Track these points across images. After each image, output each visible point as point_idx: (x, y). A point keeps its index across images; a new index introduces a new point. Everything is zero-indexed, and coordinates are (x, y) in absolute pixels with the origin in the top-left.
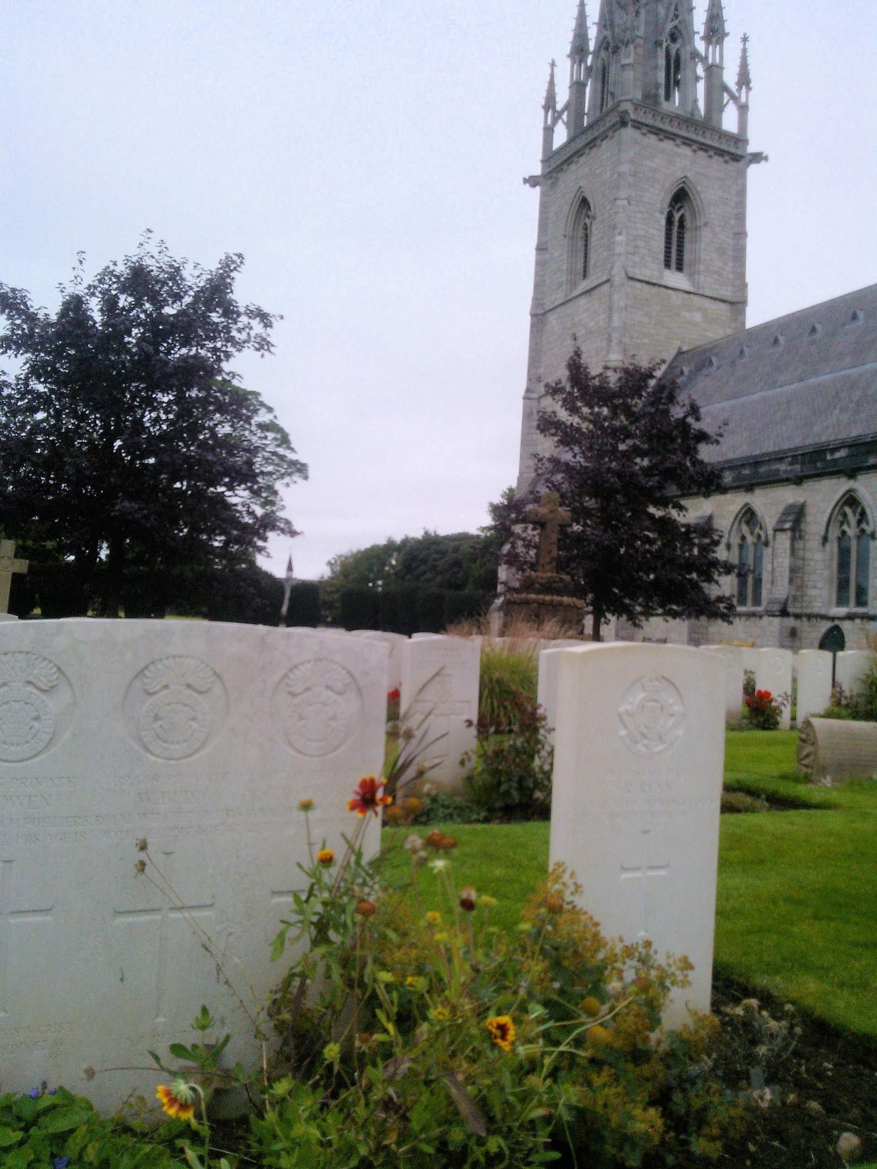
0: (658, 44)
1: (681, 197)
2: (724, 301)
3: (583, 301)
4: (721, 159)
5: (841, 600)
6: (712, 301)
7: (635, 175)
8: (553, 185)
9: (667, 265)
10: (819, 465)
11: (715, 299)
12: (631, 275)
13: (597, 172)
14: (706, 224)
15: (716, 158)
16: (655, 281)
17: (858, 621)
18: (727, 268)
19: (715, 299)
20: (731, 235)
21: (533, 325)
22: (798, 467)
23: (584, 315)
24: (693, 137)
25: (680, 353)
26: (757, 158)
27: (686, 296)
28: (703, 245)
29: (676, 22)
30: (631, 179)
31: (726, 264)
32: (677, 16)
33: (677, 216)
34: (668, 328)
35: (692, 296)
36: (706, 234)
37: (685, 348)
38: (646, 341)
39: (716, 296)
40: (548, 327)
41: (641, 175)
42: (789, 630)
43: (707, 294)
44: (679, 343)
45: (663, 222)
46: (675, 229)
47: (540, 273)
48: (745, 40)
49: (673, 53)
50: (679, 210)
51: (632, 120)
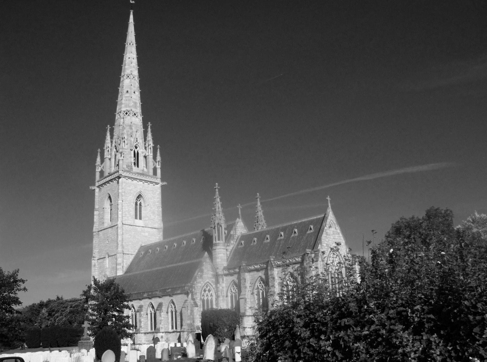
0: (131, 150)
1: (139, 196)
2: (155, 228)
3: (110, 230)
5: (173, 328)
6: (151, 229)
9: (136, 218)
10: (165, 293)
11: (152, 228)
12: (124, 223)
13: (113, 189)
16: (132, 224)
17: (175, 333)
19: (152, 228)
20: (156, 208)
22: (161, 293)
23: (110, 234)
24: (143, 179)
25: (141, 247)
27: (143, 228)
29: (137, 143)
31: (155, 217)
32: (137, 141)
33: (139, 203)
35: (144, 228)
37: (143, 245)
38: (131, 243)
39: (153, 227)
40: (100, 236)
41: (126, 192)
42: (161, 336)
43: (149, 227)
44: (140, 243)
45: (134, 206)
46: (138, 207)
49: (136, 152)
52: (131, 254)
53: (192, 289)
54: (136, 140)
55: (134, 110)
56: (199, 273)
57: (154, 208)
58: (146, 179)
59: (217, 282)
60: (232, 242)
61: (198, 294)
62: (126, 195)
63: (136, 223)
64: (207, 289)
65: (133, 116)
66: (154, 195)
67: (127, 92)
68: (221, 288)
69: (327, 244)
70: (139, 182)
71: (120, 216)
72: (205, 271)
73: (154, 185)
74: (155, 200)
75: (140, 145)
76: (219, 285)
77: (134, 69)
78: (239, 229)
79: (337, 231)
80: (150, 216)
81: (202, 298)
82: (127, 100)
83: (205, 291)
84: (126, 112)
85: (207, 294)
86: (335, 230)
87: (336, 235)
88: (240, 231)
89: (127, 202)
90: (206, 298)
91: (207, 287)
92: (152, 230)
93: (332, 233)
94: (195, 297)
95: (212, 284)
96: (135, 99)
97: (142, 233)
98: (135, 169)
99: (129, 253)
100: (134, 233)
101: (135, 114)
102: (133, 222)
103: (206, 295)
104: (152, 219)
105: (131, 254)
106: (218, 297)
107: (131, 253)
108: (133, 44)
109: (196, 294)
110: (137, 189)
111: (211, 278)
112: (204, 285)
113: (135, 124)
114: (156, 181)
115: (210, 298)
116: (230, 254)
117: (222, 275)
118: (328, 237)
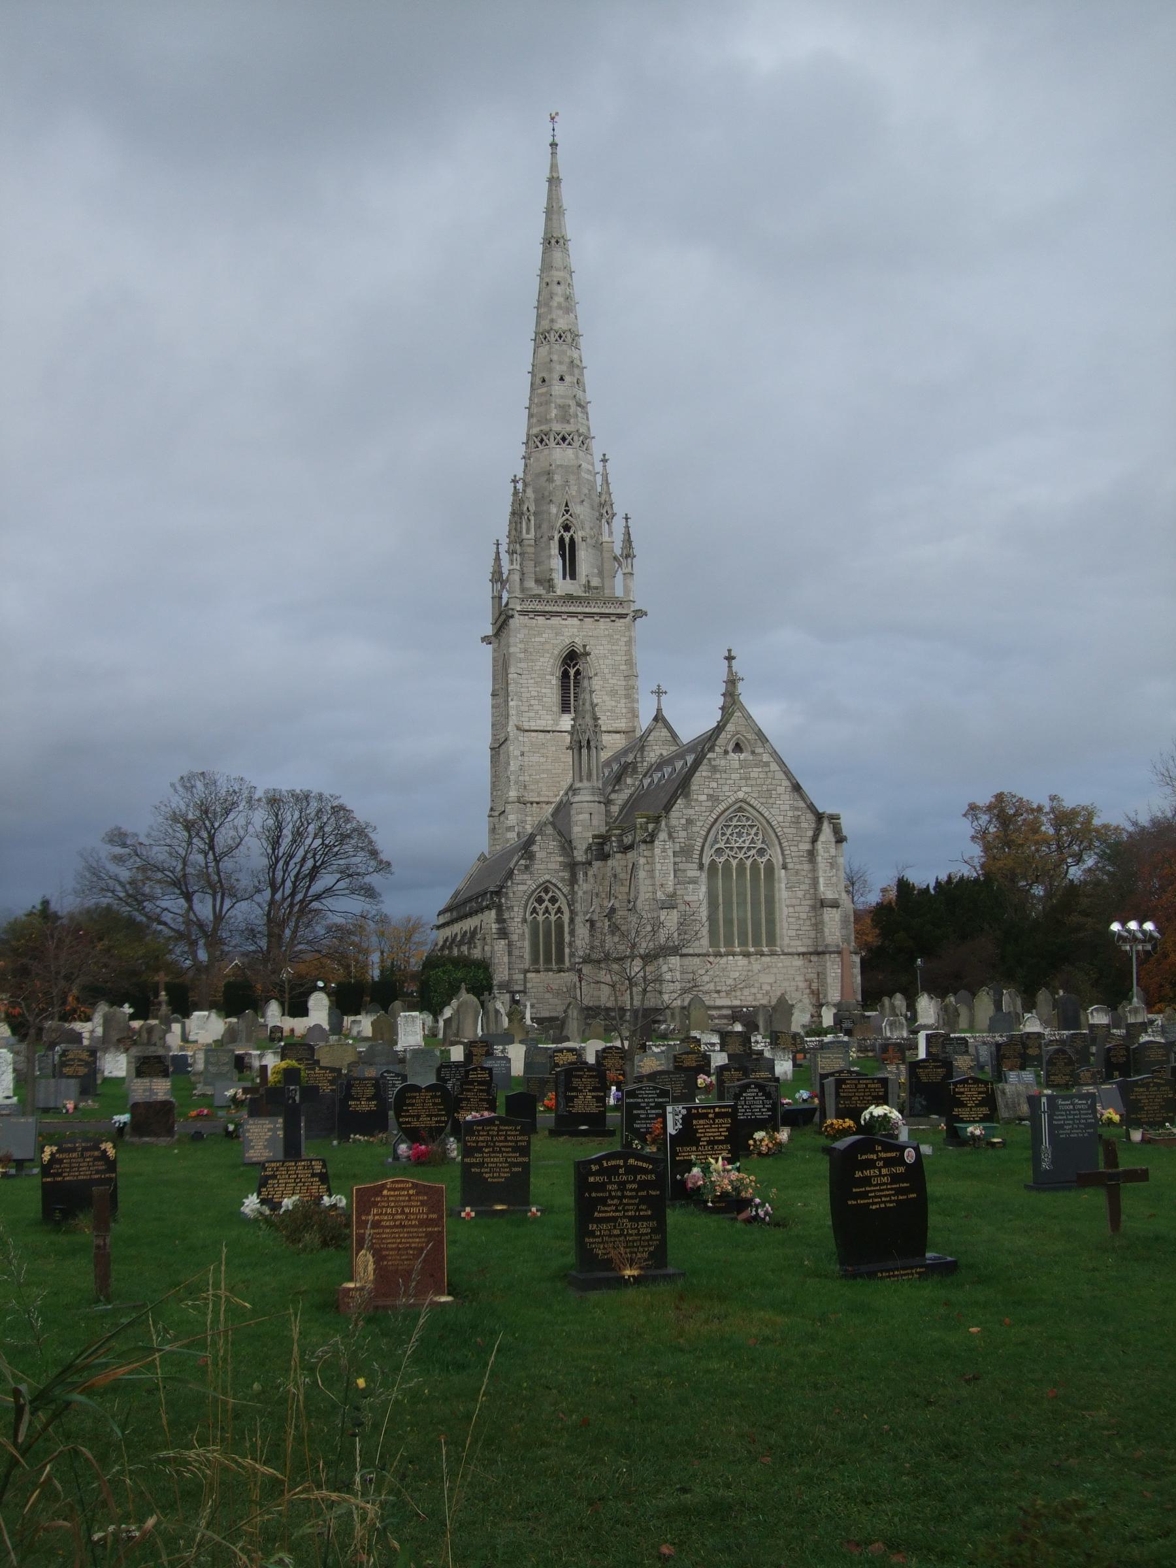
1: (572, 655)
4: (608, 620)
7: (525, 651)
8: (499, 643)
12: (527, 728)
14: (596, 675)
15: (602, 620)
16: (549, 729)
20: (622, 678)
21: (492, 757)
24: (579, 610)
26: (640, 614)
30: (522, 655)
32: (567, 511)
33: (572, 672)
34: (564, 762)
36: (596, 683)
39: (611, 729)
45: (555, 681)
47: (496, 714)
48: (627, 519)
49: (567, 540)
52: (548, 803)
53: (500, 899)
54: (563, 508)
55: (557, 427)
56: (522, 862)
57: (615, 682)
58: (587, 610)
59: (573, 881)
60: (629, 781)
61: (516, 909)
63: (561, 723)
64: (547, 898)
66: (614, 648)
67: (544, 381)
68: (580, 893)
69: (710, 797)
71: (512, 712)
72: (538, 855)
74: (618, 658)
75: (575, 522)
76: (576, 887)
77: (560, 312)
78: (654, 747)
79: (760, 758)
81: (529, 918)
82: (541, 405)
83: (540, 901)
84: (539, 438)
85: (547, 907)
86: (751, 758)
88: (658, 753)
89: (533, 676)
90: (541, 918)
91: (546, 891)
92: (610, 738)
93: (737, 766)
94: (506, 916)
95: (560, 885)
96: (562, 397)
99: (542, 799)
100: (554, 749)
101: (564, 439)
102: (552, 722)
103: (541, 912)
104: (610, 708)
105: (548, 803)
106: (573, 913)
107: (546, 799)
108: (557, 242)
109: (510, 908)
110: (562, 638)
111: (556, 871)
112: (536, 890)
113: (558, 466)
114: (619, 611)
115: (553, 918)
116: (621, 811)
117: (583, 864)
118: (718, 776)
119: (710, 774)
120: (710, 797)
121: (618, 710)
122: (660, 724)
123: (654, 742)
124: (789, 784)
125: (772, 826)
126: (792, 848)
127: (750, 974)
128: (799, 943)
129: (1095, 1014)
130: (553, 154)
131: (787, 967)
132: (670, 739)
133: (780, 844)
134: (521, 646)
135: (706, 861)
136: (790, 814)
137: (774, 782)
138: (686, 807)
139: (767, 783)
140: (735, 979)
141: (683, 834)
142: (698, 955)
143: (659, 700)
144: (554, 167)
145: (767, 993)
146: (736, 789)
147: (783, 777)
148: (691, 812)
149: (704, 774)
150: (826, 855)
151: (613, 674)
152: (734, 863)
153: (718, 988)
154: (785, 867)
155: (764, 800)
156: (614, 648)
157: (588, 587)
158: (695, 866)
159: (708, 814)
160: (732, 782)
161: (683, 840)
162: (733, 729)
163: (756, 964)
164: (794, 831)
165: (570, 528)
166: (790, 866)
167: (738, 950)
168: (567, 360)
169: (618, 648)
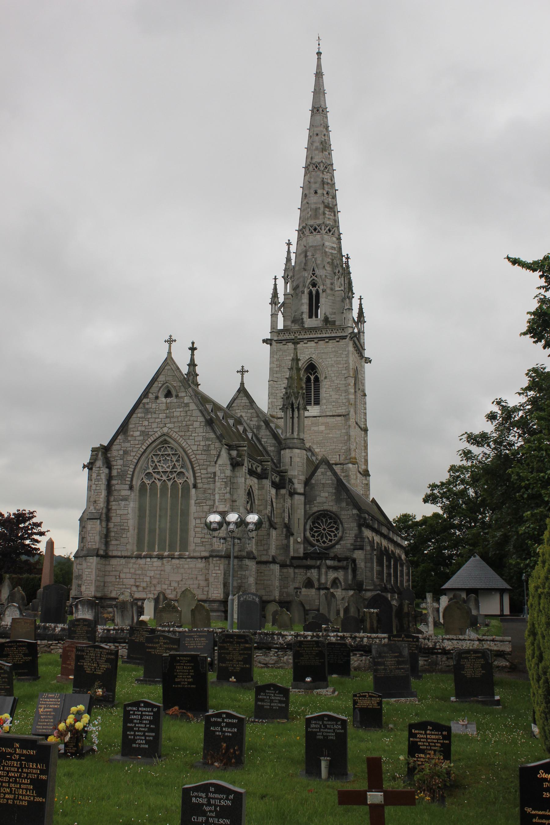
4: (334, 341)
14: (326, 378)
15: (331, 341)
18: (341, 397)
20: (343, 379)
27: (315, 418)
28: (325, 389)
30: (278, 369)
32: (314, 274)
33: (312, 378)
35: (318, 418)
39: (335, 414)
43: (328, 414)
49: (314, 292)
50: (314, 374)
51: (275, 341)
54: (311, 272)
57: (339, 382)
62: (283, 370)
65: (312, 233)
66: (338, 359)
69: (142, 432)
70: (309, 343)
73: (338, 341)
74: (341, 366)
75: (318, 280)
78: (237, 411)
80: (331, 396)
86: (175, 401)
87: (178, 410)
93: (164, 408)
96: (316, 203)
97: (313, 428)
98: (309, 323)
101: (315, 229)
104: (335, 400)
108: (318, 110)
110: (304, 356)
118: (150, 416)
119: (143, 415)
120: (142, 432)
121: (340, 401)
122: (241, 395)
123: (237, 408)
124: (204, 420)
125: (187, 454)
126: (203, 471)
127: (163, 573)
128: (203, 548)
129: (80, 607)
130: (319, 59)
131: (192, 568)
132: (249, 404)
133: (193, 468)
134: (278, 363)
135: (137, 483)
136: (202, 443)
137: (192, 418)
138: (124, 442)
139: (186, 419)
140: (151, 577)
141: (120, 462)
142: (125, 557)
143: (242, 377)
144: (319, 66)
145: (175, 589)
146: (162, 425)
147: (200, 414)
148: (128, 445)
149: (139, 415)
150: (223, 475)
151: (338, 377)
152: (159, 484)
153: (138, 584)
154: (195, 486)
155: (180, 434)
156: (338, 359)
157: (326, 320)
158: (127, 487)
159: (139, 446)
160: (159, 420)
161: (120, 467)
162: (163, 379)
163: (168, 566)
164: (205, 457)
165: (316, 284)
166: (199, 485)
167: (155, 553)
168: (320, 180)
169: (341, 359)
